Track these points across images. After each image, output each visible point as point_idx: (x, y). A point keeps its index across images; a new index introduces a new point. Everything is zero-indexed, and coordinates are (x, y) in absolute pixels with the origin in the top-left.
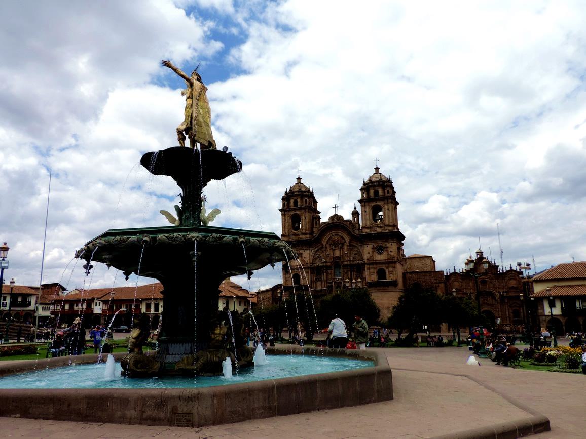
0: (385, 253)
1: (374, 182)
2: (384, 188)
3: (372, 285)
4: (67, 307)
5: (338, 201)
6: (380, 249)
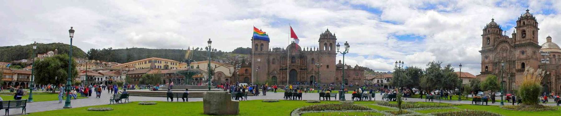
0: (525, 55)
2: (527, 19)
6: (523, 53)
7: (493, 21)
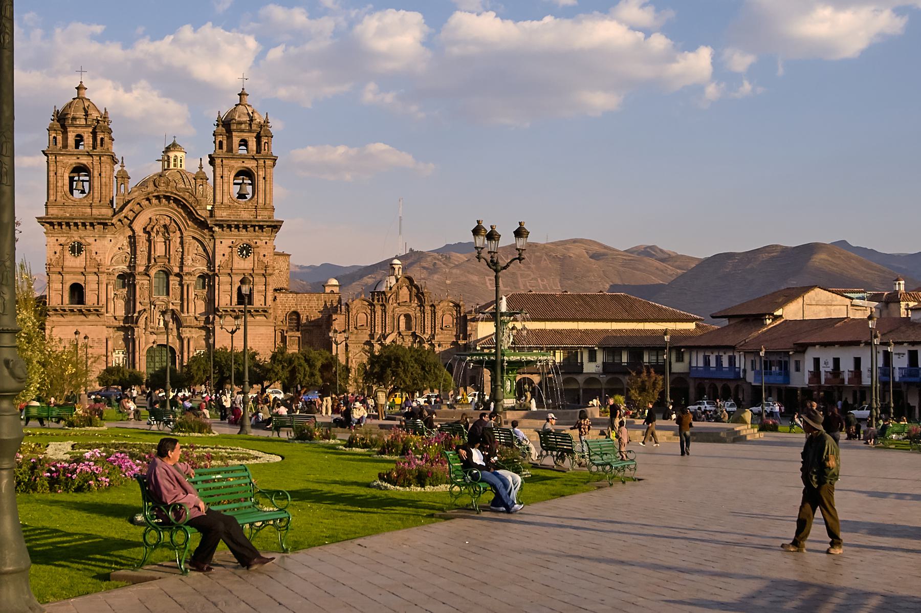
1: (240, 123)
6: (246, 250)
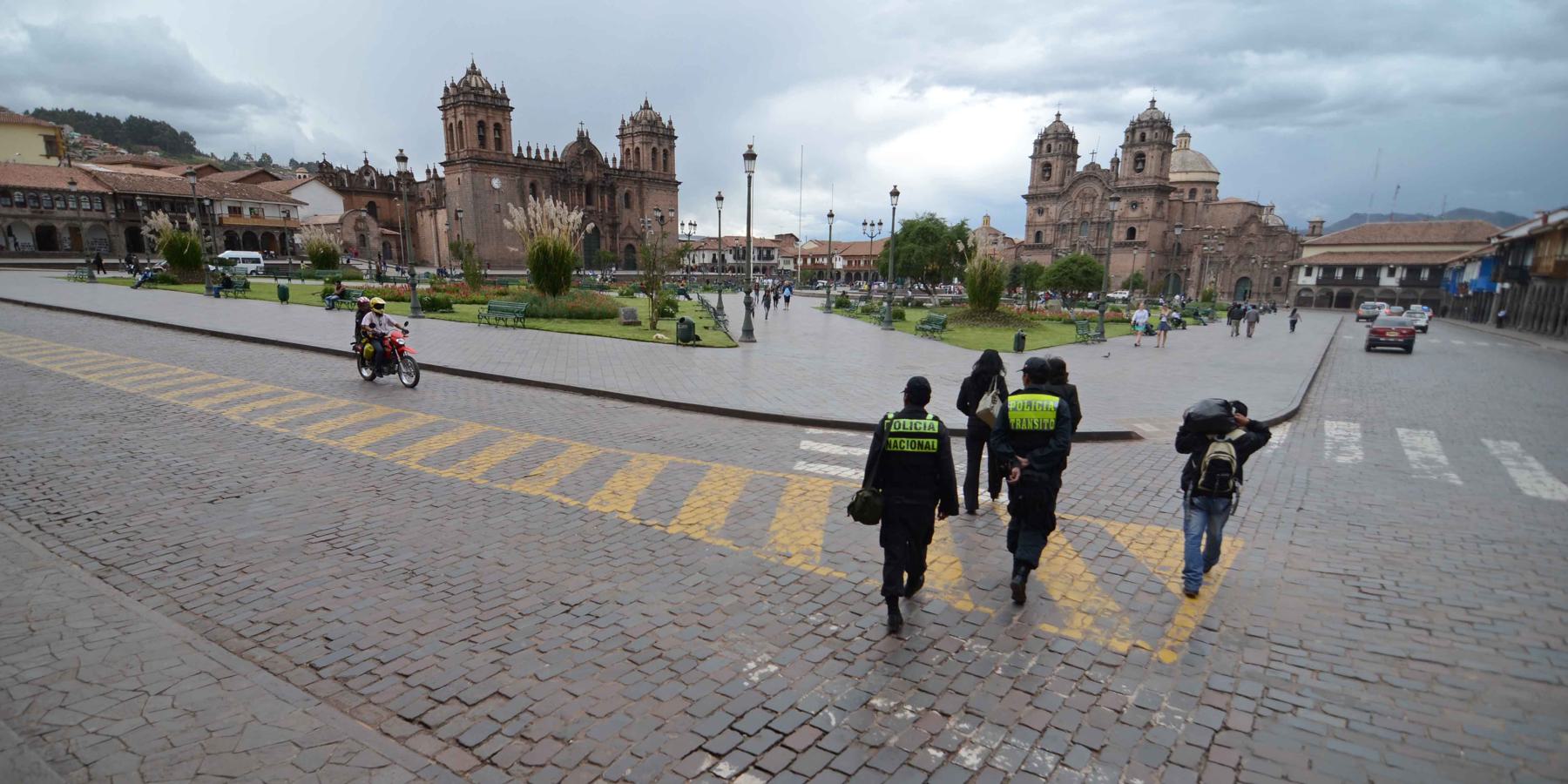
3: (1120, 245)
4: (800, 262)
5: (1099, 145)
6: (1134, 205)
7: (1058, 121)
